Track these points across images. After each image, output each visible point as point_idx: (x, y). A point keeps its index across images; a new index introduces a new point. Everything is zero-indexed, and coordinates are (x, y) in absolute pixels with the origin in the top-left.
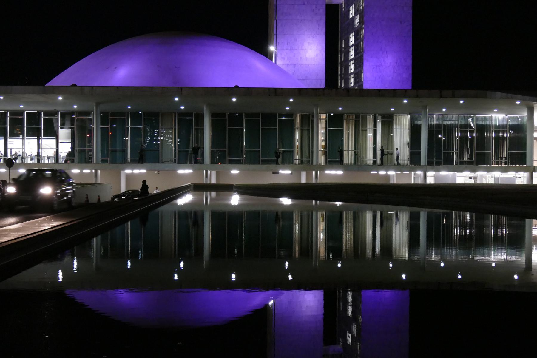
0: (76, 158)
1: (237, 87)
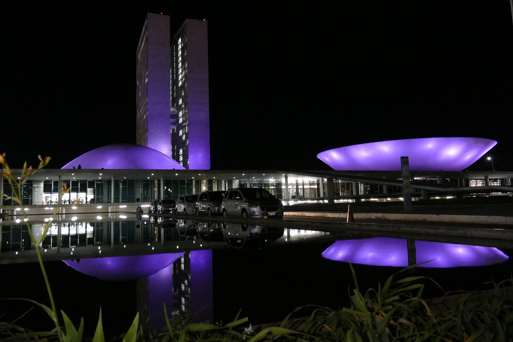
0: (96, 201)
1: (174, 169)
